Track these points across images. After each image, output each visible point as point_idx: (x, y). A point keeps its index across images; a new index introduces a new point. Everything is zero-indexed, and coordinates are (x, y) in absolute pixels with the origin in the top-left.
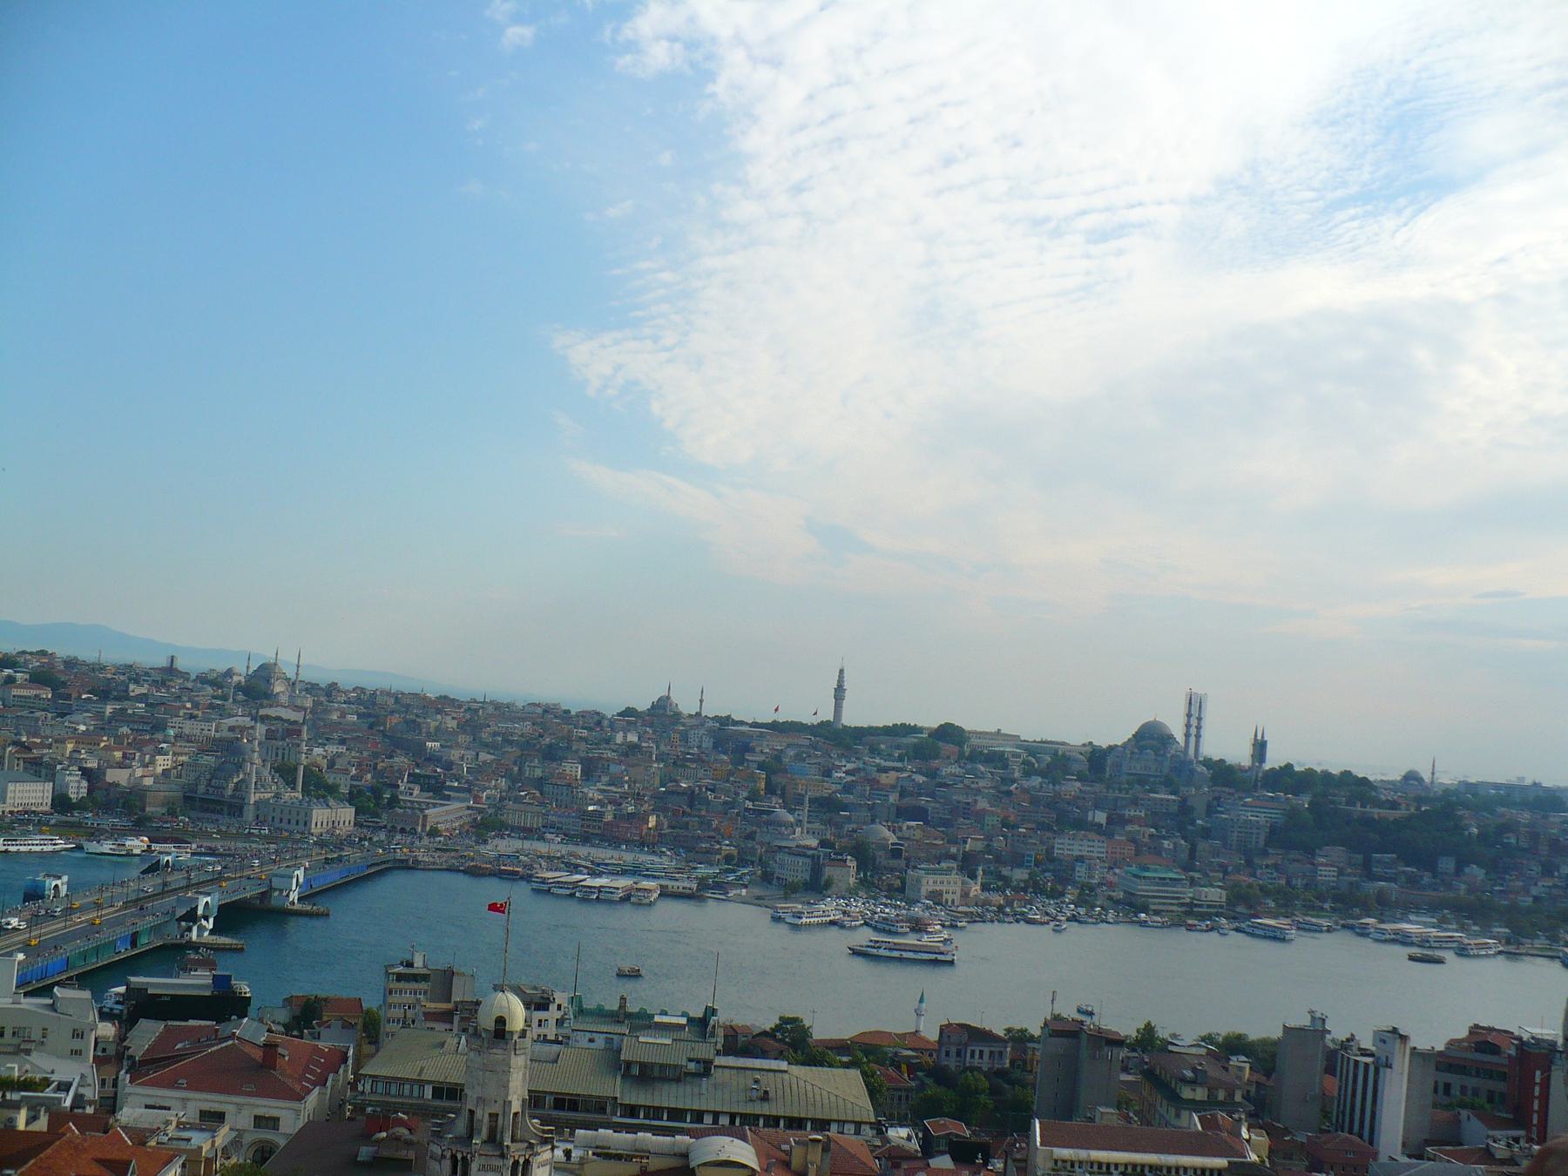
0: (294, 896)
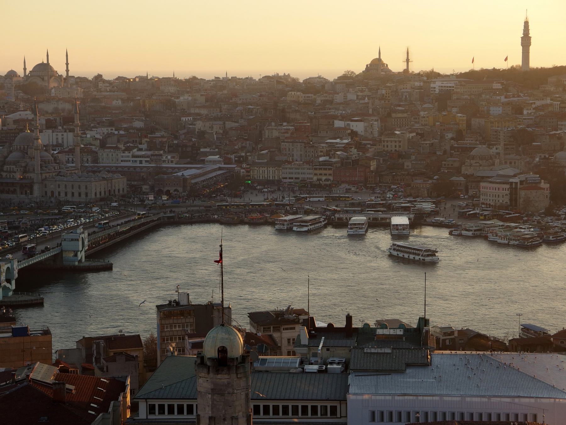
0: (81, 255)
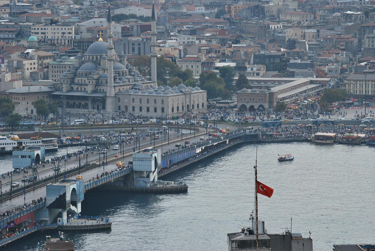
0: (154, 176)
